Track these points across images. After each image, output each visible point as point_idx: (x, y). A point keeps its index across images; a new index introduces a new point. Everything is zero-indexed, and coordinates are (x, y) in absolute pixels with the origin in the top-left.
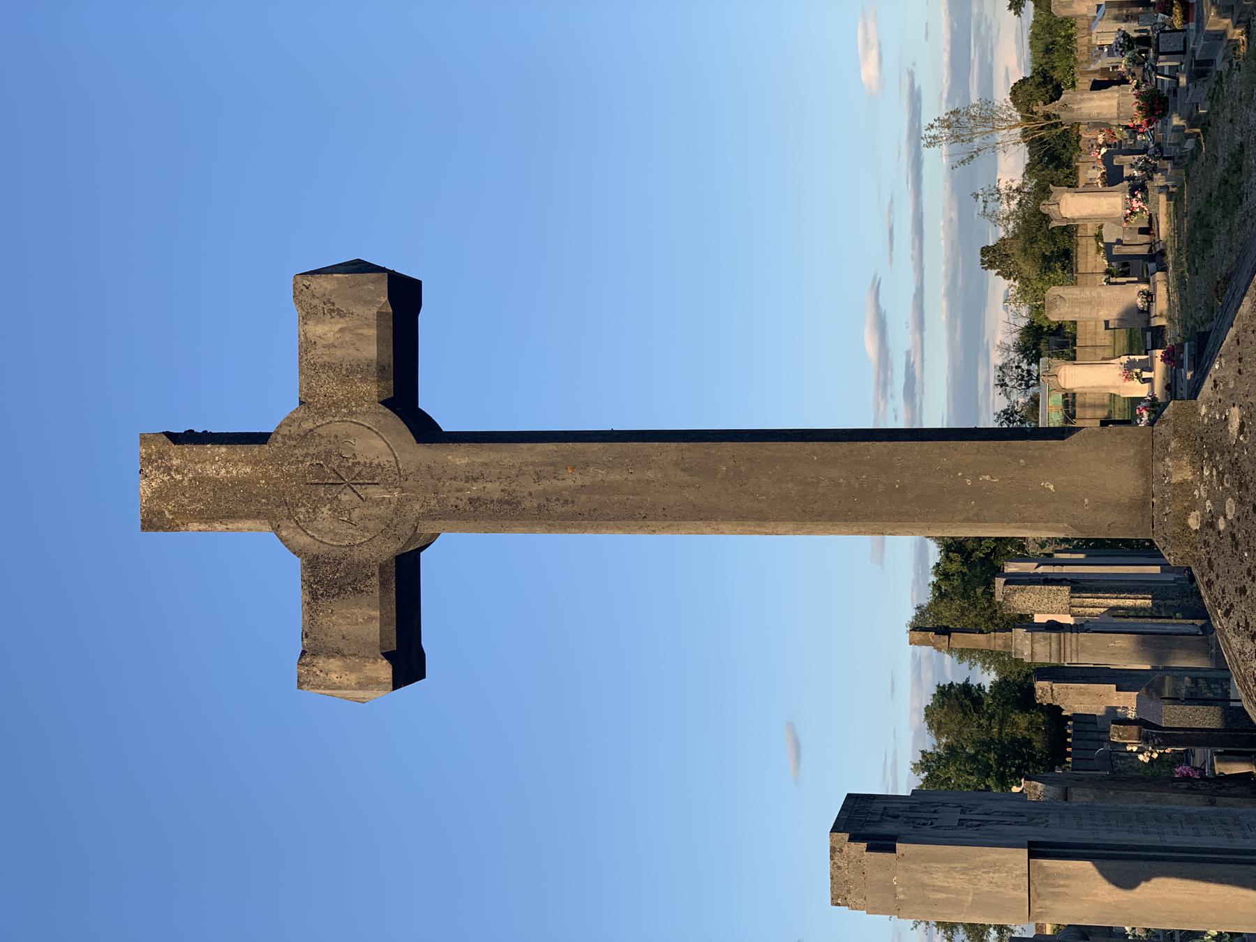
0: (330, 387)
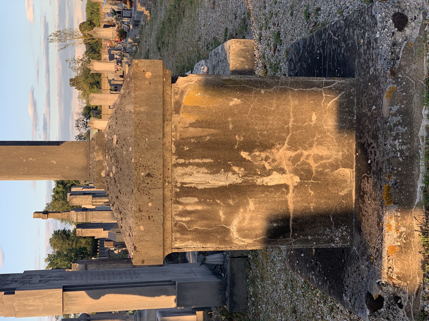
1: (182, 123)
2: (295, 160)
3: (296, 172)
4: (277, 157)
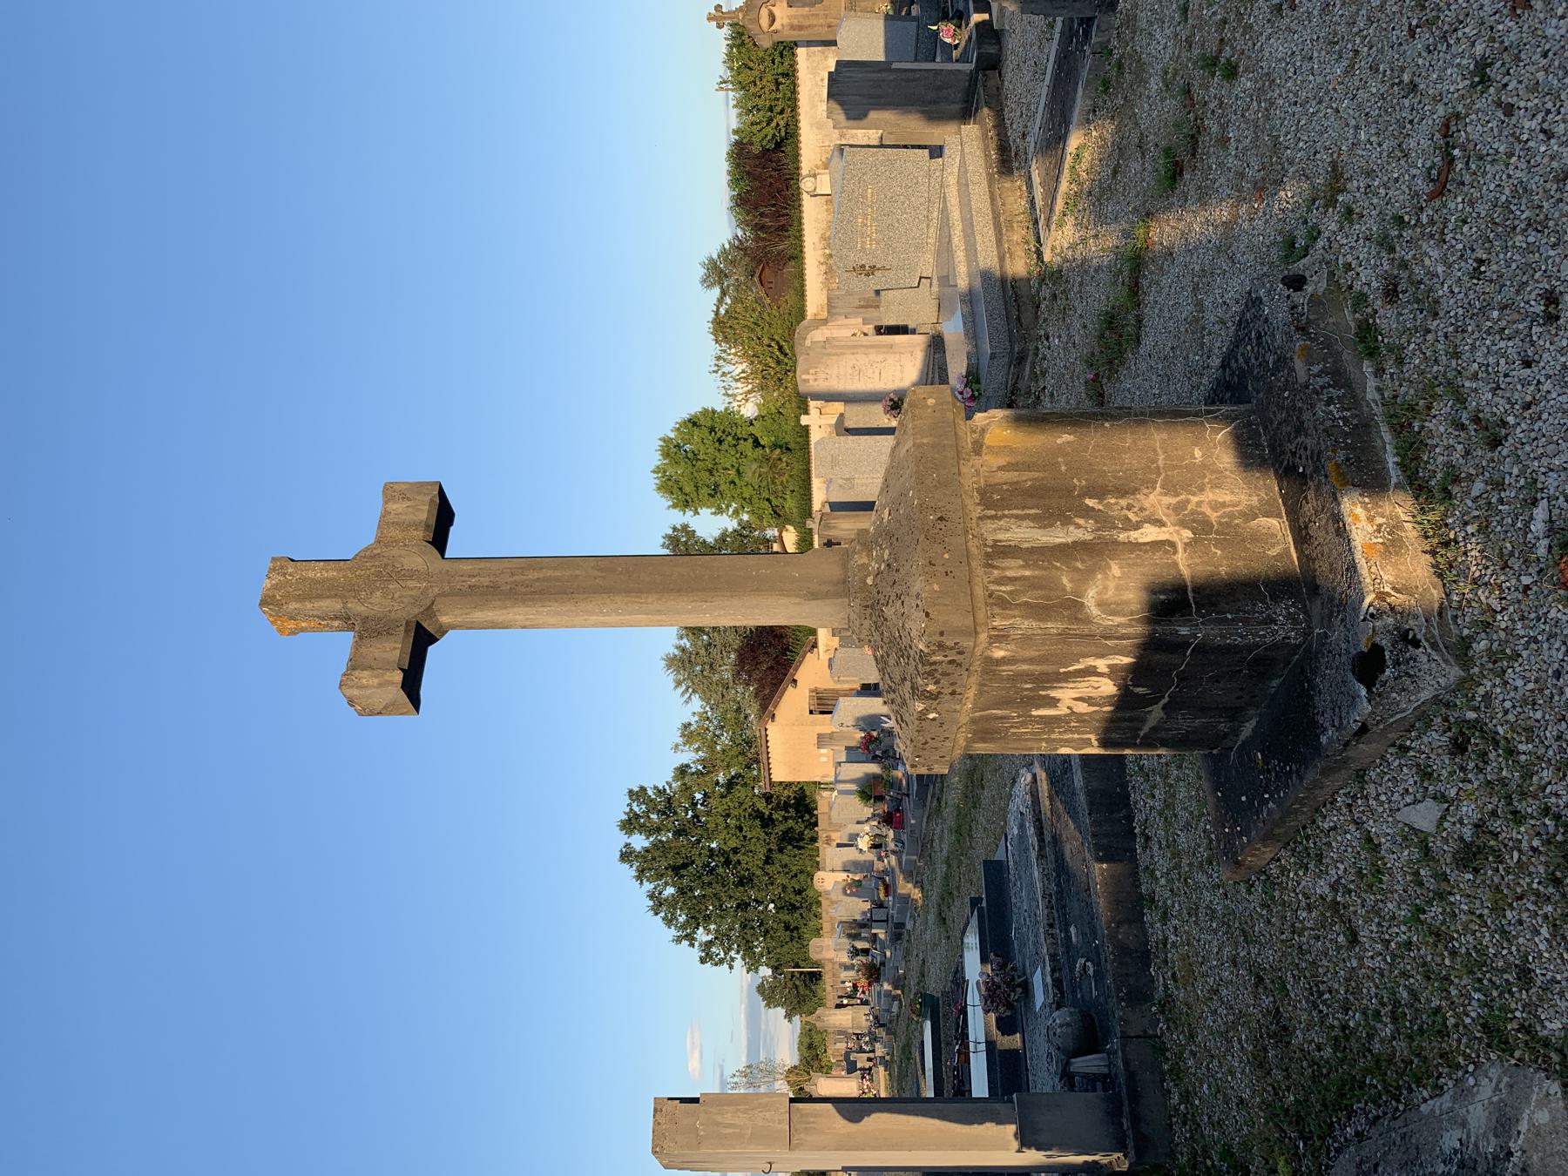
0: (395, 533)
1: (987, 467)
2: (1179, 508)
3: (1183, 524)
4: (1147, 505)
